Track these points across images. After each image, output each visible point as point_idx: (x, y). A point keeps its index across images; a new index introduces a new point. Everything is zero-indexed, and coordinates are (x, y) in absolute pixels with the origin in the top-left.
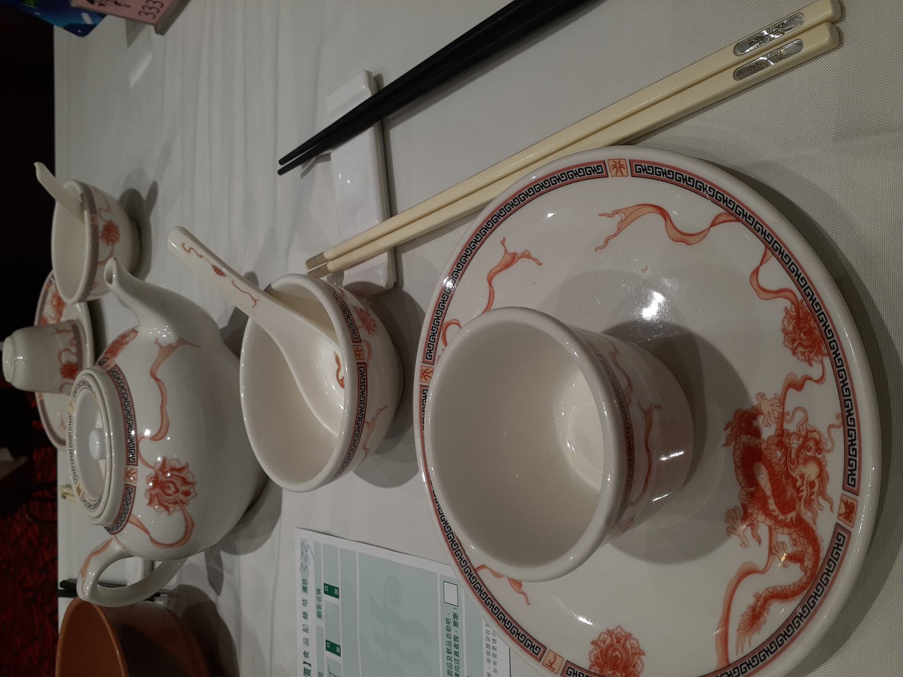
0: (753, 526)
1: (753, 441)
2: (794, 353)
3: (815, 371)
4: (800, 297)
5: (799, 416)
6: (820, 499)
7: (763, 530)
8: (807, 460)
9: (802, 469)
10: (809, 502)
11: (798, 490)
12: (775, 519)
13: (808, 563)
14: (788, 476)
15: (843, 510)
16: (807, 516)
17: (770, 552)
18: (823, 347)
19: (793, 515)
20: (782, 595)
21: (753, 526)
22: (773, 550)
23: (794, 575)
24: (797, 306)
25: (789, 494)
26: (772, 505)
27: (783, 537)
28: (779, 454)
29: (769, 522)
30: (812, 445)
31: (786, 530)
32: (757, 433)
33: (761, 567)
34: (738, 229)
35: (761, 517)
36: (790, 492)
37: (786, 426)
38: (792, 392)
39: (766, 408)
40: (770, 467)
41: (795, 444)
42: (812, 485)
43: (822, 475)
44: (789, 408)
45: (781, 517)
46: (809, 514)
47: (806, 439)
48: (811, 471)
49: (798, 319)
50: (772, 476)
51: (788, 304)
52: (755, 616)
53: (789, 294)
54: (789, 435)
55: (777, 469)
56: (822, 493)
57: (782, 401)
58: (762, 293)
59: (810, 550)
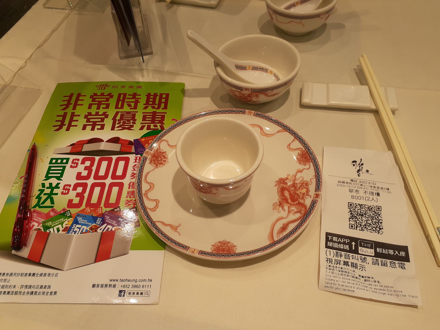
0: (283, 207)
1: (284, 186)
2: (300, 163)
3: (307, 166)
4: (304, 149)
5: (301, 179)
6: (307, 197)
7: (286, 208)
8: (303, 188)
9: (300, 191)
10: (303, 198)
11: (299, 196)
12: (291, 204)
13: (303, 212)
14: (296, 193)
15: (315, 196)
16: (302, 201)
17: (289, 212)
18: (310, 160)
19: (297, 202)
20: (294, 221)
21: (283, 207)
22: (289, 212)
23: (298, 215)
24: (303, 152)
25: (295, 198)
26: (289, 201)
27: (294, 208)
28: (293, 189)
29: (288, 205)
30: (305, 185)
31: (294, 206)
32: (286, 184)
33: (285, 217)
34: (287, 134)
35: (285, 204)
36: (296, 197)
37: (296, 182)
38: (299, 173)
39: (289, 178)
40: (289, 191)
41: (299, 186)
42: (304, 194)
43: (308, 191)
44: (297, 177)
45: (293, 203)
46: (303, 201)
47: (303, 183)
48: (304, 191)
49: (302, 155)
50: (290, 194)
51: (299, 152)
52: (284, 228)
53: (301, 149)
54: (297, 184)
55: (292, 192)
56: (308, 195)
57: (295, 176)
58: (291, 150)
59: (303, 209)
